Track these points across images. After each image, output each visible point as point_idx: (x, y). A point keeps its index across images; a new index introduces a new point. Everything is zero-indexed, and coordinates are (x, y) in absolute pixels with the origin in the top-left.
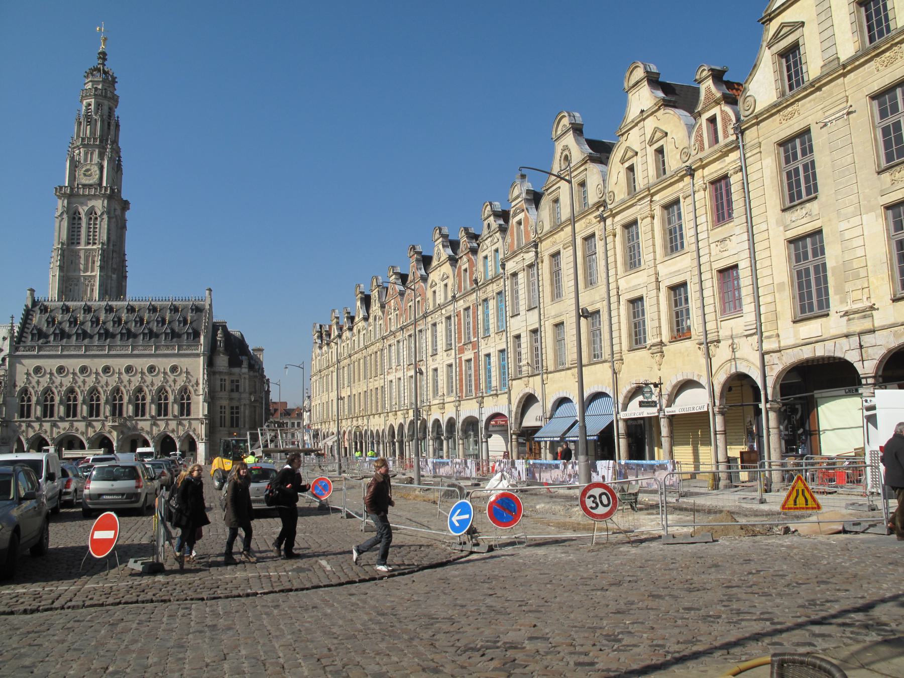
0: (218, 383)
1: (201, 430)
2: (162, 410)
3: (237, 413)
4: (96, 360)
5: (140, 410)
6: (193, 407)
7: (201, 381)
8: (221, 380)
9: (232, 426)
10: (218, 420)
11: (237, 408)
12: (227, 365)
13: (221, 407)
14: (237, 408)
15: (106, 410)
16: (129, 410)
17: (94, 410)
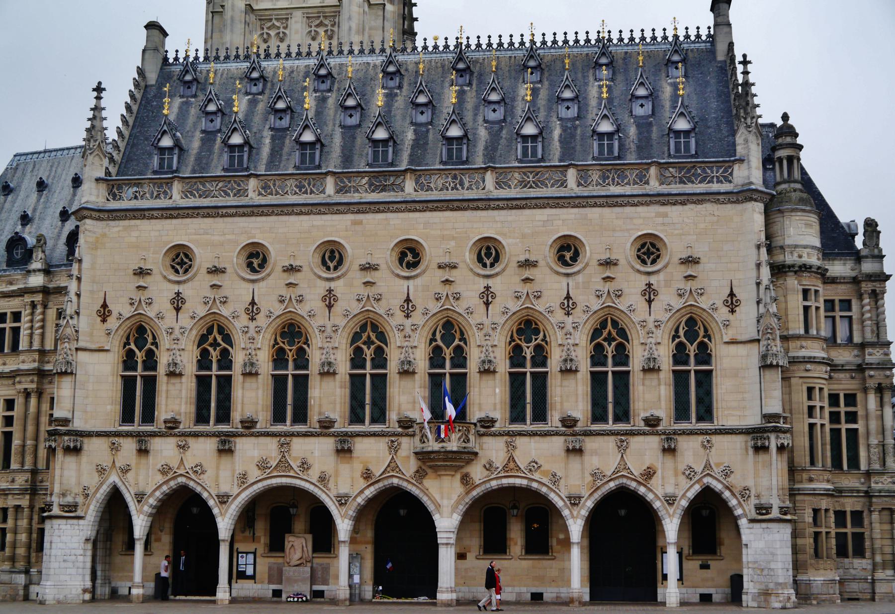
0: (796, 303)
1: (757, 479)
2: (611, 399)
3: (852, 417)
4: (371, 219)
5: (529, 399)
6: (721, 389)
7: (746, 295)
8: (806, 292)
9: (837, 463)
10: (803, 442)
11: (851, 399)
12: (818, 245)
13: (810, 390)
14: (851, 399)
15: (409, 399)
16: (488, 398)
17: (368, 399)
